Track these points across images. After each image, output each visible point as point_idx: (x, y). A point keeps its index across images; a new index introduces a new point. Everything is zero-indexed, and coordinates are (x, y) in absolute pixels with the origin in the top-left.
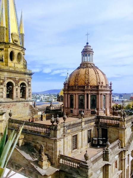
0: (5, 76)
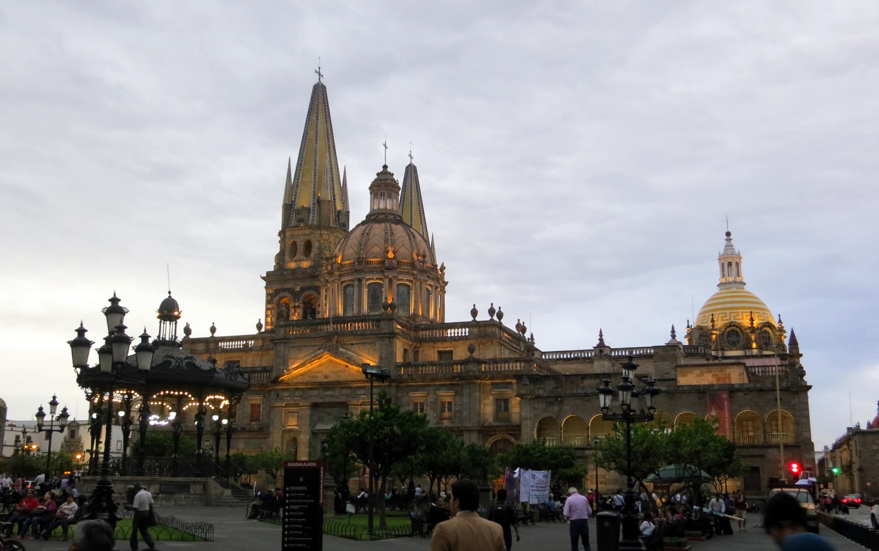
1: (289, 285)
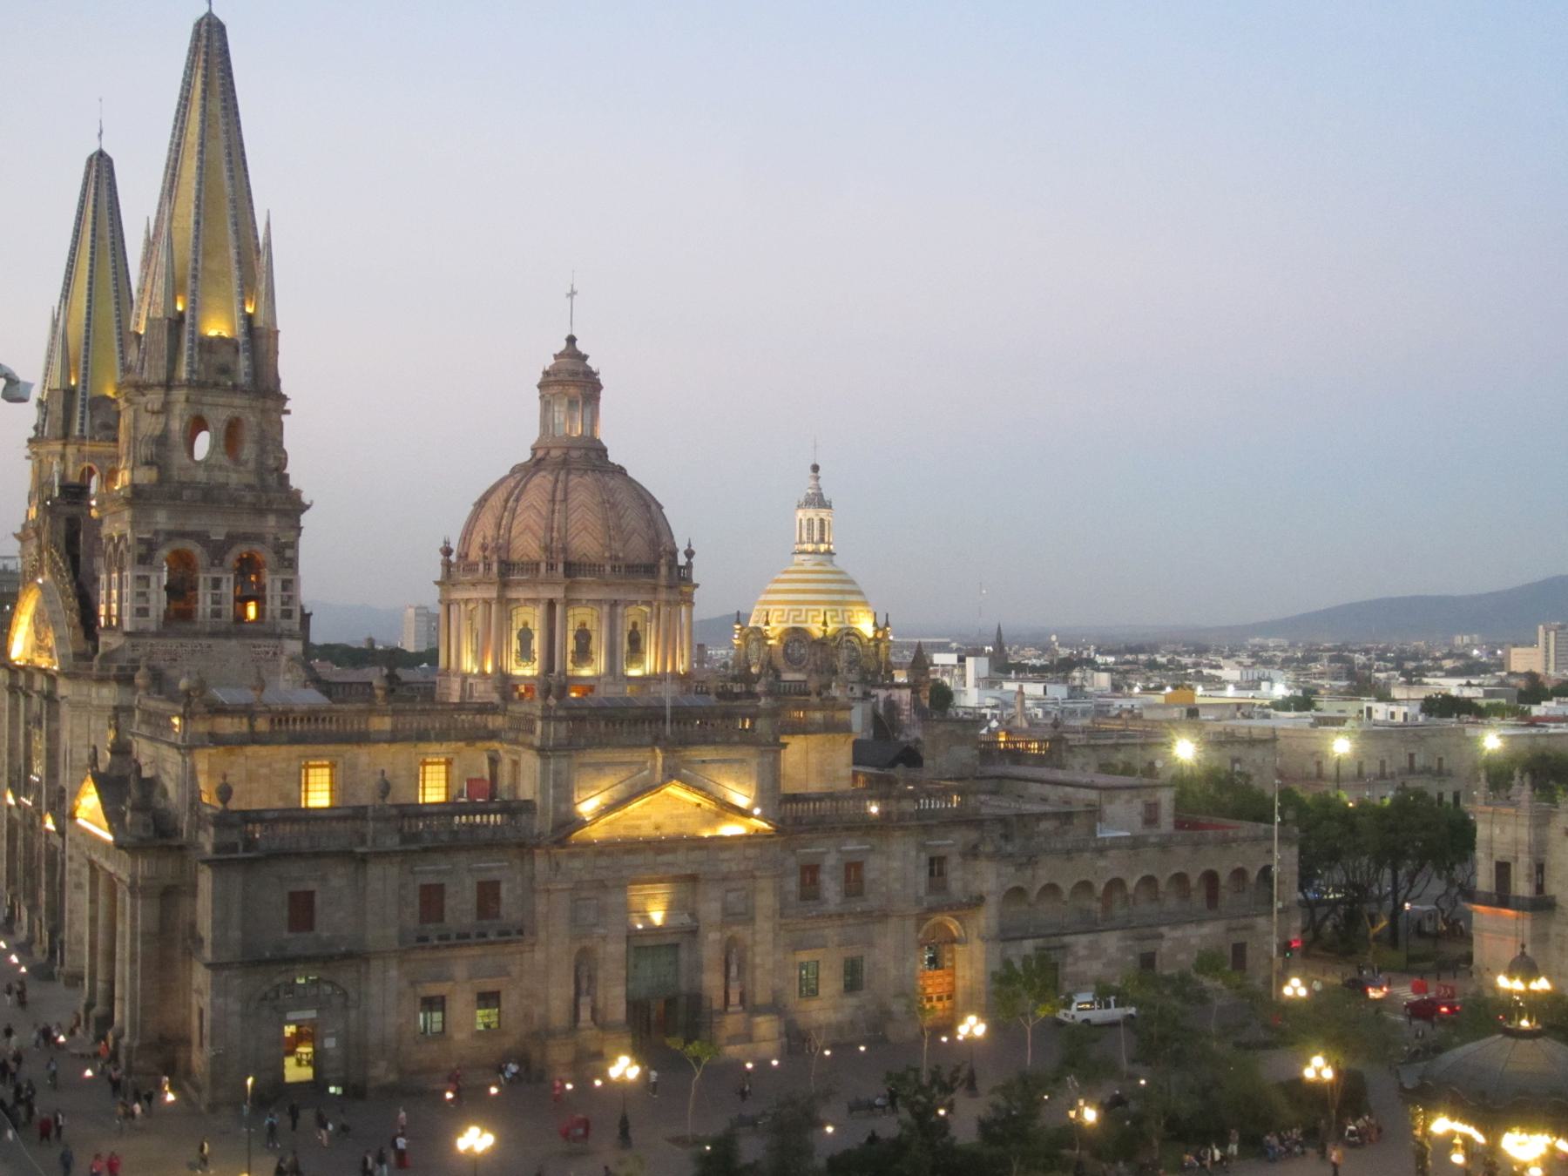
0: (159, 527)
1: (193, 524)
